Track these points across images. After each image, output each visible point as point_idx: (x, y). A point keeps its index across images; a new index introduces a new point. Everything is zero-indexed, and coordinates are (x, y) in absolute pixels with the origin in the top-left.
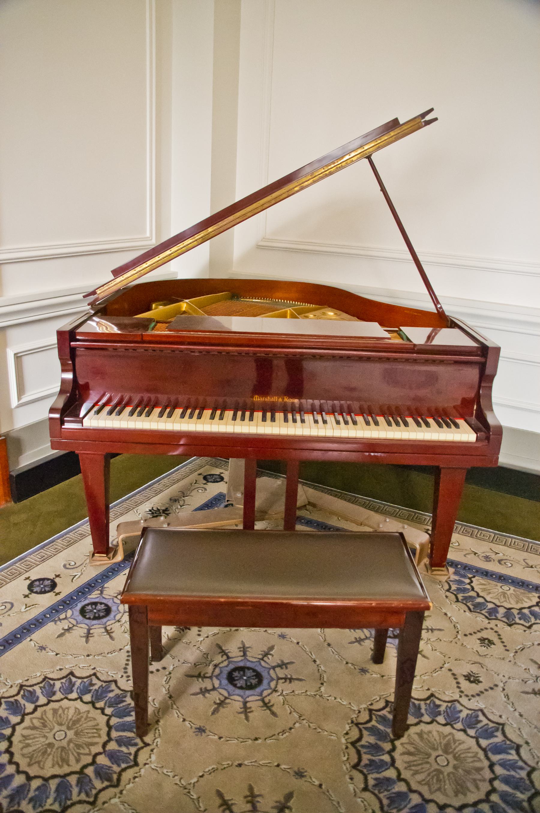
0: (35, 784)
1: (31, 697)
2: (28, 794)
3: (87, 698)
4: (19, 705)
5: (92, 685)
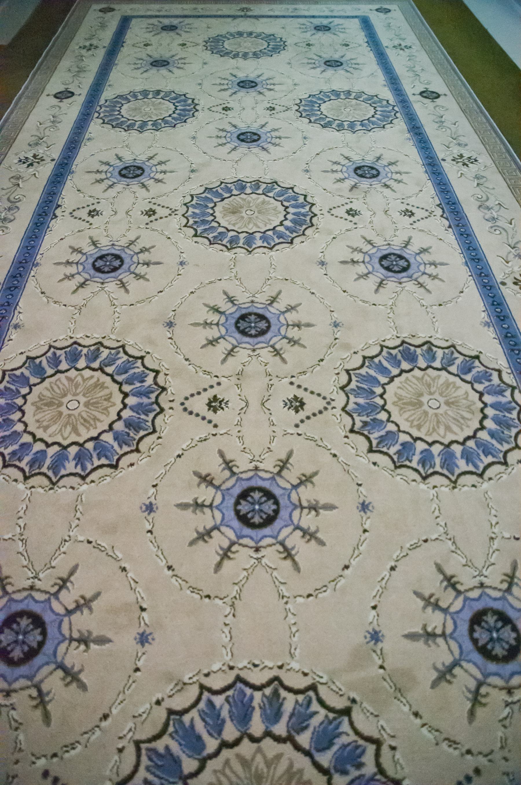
0: (480, 387)
1: (426, 459)
2: (489, 386)
3: (383, 416)
4: (443, 461)
5: (365, 424)
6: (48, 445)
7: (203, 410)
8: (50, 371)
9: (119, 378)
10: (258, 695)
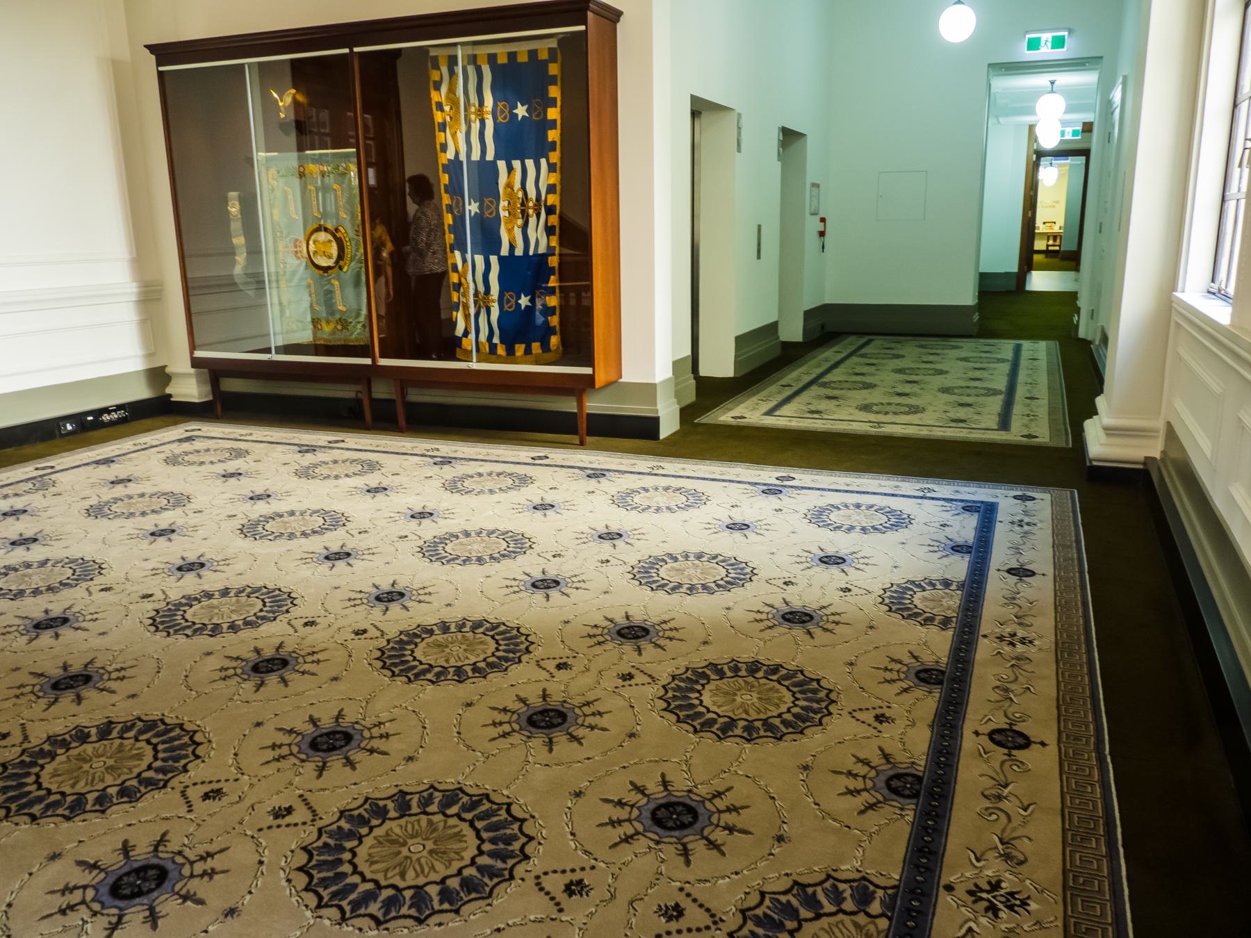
6: (719, 716)
7: (871, 720)
8: (729, 674)
9: (795, 689)
10: (880, 893)
